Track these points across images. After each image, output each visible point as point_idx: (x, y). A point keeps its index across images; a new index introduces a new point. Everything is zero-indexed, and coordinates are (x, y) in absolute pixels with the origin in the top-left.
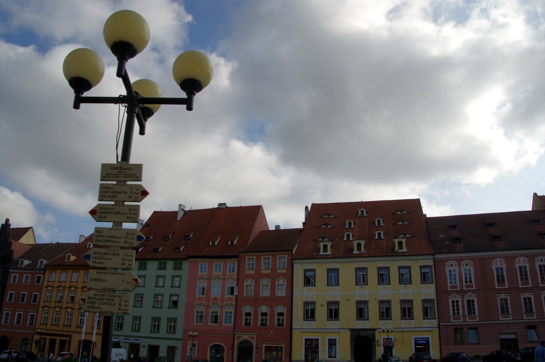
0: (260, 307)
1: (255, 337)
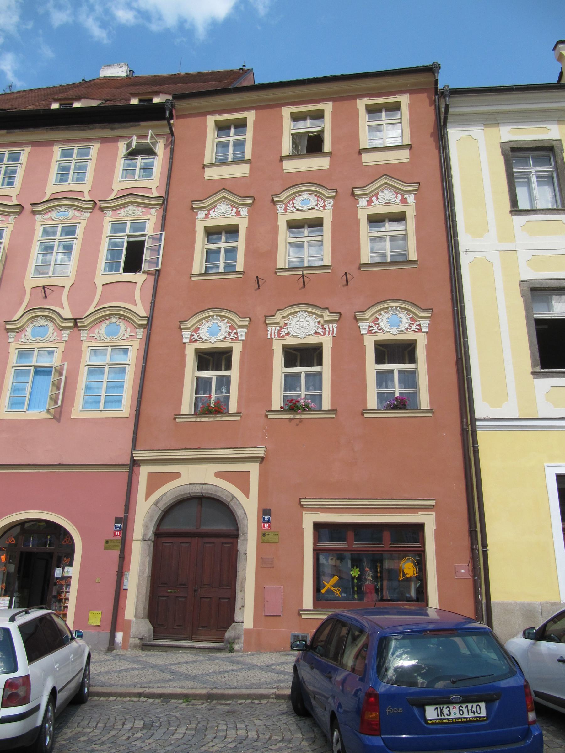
0: (279, 315)
1: (254, 469)
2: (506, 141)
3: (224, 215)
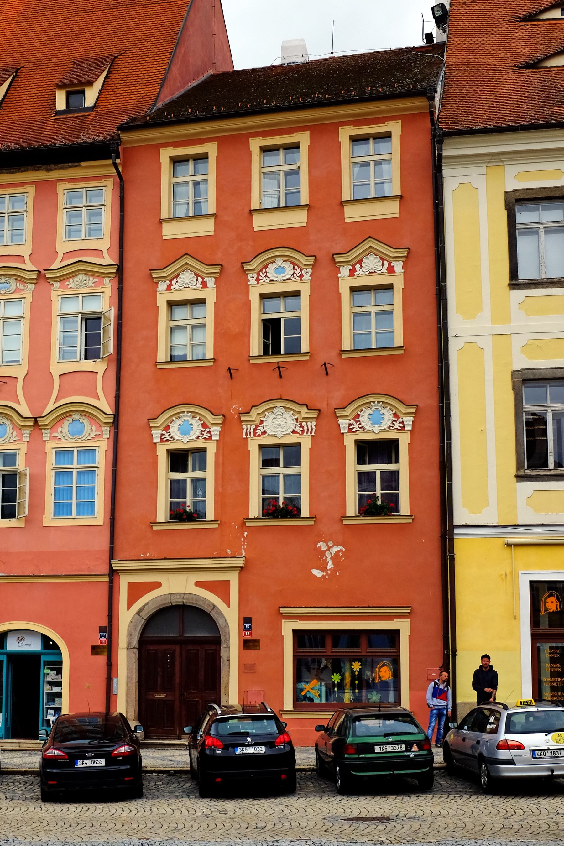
0: (254, 413)
1: (234, 578)
2: (512, 190)
3: (189, 287)
